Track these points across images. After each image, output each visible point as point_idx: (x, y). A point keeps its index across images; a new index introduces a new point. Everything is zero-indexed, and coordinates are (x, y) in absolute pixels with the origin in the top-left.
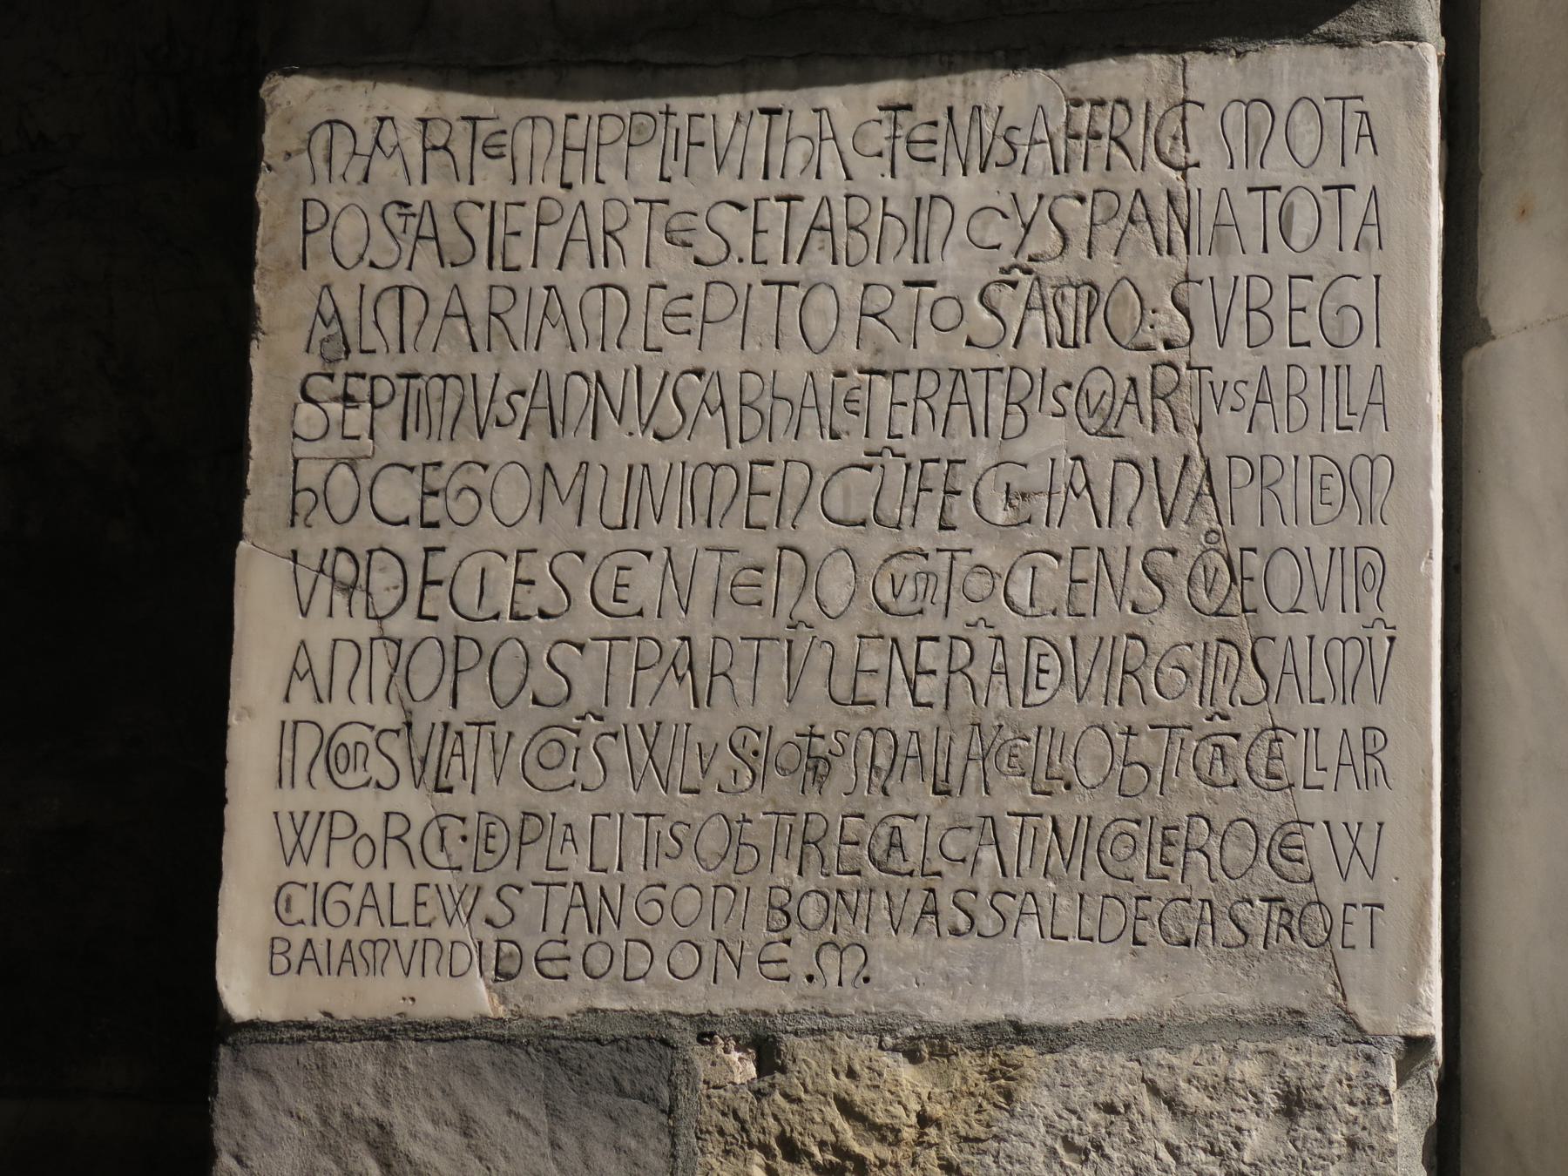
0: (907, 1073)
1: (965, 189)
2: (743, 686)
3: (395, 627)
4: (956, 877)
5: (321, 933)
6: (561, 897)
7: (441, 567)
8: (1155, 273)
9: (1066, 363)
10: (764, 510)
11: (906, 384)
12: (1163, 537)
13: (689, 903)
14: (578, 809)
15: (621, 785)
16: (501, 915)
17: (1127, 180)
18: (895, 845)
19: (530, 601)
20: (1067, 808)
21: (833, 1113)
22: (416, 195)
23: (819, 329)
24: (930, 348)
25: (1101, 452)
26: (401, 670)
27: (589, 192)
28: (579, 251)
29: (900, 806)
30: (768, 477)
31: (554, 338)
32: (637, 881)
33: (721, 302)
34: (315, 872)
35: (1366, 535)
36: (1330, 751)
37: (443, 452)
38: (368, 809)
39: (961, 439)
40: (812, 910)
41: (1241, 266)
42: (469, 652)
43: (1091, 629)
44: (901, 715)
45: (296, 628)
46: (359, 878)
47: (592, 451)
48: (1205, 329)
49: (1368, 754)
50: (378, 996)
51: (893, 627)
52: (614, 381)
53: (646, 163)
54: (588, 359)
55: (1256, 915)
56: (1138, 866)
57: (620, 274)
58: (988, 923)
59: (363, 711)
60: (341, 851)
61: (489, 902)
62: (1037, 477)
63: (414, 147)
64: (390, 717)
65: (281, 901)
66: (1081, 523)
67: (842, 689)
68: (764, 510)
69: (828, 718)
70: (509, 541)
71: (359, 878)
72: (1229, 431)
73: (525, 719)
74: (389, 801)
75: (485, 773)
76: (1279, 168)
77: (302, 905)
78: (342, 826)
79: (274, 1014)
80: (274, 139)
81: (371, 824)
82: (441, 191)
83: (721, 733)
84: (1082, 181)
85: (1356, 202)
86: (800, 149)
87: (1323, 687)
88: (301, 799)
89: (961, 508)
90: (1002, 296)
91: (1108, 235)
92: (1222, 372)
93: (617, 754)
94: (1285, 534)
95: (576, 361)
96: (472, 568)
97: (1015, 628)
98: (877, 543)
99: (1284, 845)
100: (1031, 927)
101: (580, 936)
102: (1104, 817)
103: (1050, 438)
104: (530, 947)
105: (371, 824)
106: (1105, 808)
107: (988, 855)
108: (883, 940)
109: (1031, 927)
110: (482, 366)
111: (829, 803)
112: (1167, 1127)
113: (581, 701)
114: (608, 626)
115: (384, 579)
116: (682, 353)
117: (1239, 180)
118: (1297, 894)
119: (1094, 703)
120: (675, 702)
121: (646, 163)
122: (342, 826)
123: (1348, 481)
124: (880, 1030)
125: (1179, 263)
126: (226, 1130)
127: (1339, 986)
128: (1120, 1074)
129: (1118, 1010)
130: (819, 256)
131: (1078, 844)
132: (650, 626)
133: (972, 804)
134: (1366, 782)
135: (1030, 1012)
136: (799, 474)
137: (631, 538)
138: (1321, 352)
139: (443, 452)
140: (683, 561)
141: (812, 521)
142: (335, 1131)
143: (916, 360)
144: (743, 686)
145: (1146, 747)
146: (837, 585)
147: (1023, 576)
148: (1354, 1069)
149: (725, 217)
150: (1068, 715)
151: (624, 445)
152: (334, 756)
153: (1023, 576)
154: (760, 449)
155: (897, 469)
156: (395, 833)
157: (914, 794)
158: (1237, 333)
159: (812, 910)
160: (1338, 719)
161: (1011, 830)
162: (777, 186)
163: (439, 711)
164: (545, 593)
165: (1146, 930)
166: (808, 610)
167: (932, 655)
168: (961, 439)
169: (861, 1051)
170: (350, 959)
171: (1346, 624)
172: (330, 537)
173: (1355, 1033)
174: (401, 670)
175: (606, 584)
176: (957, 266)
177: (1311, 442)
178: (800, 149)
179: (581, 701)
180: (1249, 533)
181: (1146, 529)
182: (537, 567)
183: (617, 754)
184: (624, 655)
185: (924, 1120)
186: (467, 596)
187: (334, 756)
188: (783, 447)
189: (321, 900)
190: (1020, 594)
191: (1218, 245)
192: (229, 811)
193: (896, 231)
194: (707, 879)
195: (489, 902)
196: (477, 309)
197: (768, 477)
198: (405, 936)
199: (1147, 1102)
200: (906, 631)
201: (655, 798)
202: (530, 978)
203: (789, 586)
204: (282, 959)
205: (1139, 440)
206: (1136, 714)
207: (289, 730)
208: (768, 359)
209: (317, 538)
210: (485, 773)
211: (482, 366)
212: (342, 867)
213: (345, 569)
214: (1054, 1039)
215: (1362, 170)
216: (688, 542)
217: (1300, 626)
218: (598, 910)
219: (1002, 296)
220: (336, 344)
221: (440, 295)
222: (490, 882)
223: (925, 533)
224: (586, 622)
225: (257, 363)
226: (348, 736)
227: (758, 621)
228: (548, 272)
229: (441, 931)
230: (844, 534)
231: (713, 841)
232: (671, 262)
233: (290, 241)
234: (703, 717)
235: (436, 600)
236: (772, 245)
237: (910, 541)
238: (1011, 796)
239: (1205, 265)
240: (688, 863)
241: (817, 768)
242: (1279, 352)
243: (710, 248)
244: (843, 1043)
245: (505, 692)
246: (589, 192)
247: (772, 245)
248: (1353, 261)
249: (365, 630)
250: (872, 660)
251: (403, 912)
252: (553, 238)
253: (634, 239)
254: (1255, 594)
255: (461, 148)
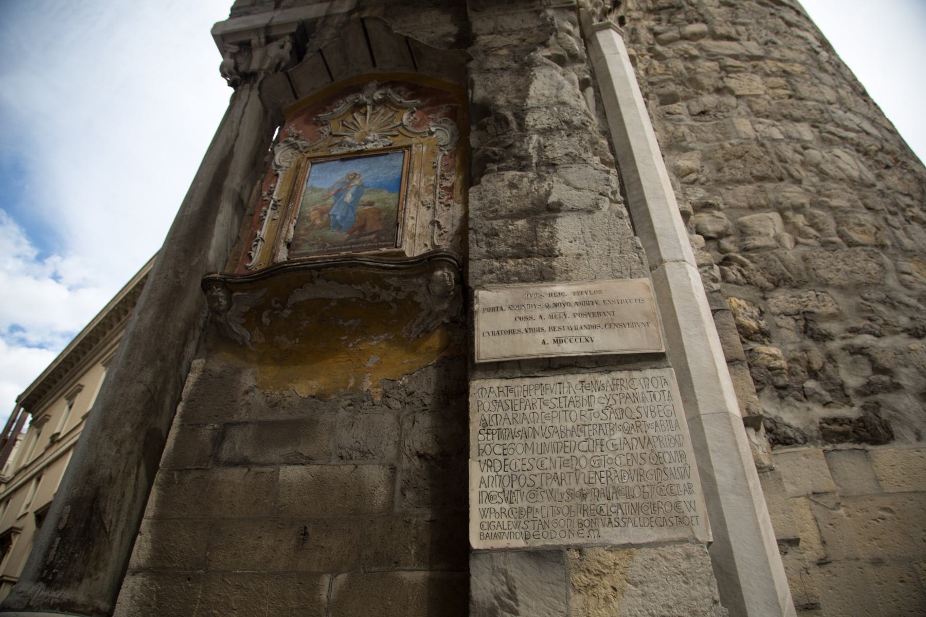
0: (610, 554)
1: (597, 394)
2: (568, 481)
3: (500, 473)
4: (614, 516)
5: (490, 531)
6: (537, 523)
7: (507, 462)
8: (633, 406)
9: (619, 422)
10: (567, 450)
11: (591, 427)
12: (643, 451)
13: (562, 523)
14: (538, 506)
15: (546, 501)
16: (525, 526)
17: (625, 391)
18: (601, 510)
19: (525, 468)
20: (634, 501)
21: (597, 563)
22: (498, 399)
23: (573, 418)
24: (594, 421)
25: (629, 437)
26: (502, 481)
27: (528, 397)
28: (528, 407)
29: (601, 502)
30: (568, 444)
31: (525, 422)
32: (551, 519)
33: (555, 415)
34: (488, 519)
35: (680, 449)
36: (682, 488)
37: (506, 442)
38: (497, 507)
39: (602, 436)
40: (587, 523)
41: (648, 404)
42: (514, 477)
43: (633, 468)
44: (598, 486)
45: (481, 474)
46: (497, 521)
47: (534, 441)
48: (644, 415)
49: (689, 488)
50: (502, 543)
51: (595, 469)
52: (537, 428)
53: (539, 392)
54: (531, 425)
55: (674, 520)
56: (649, 512)
57: (536, 411)
58: (622, 524)
59: (495, 489)
60: (493, 515)
61: (522, 525)
62: (617, 442)
63: (497, 392)
64: (500, 490)
65: (481, 526)
66: (627, 449)
67: (587, 481)
68: (567, 450)
69: (585, 487)
70: (520, 457)
71: (497, 521)
72: (651, 432)
73: (526, 490)
74: (501, 506)
75: (519, 500)
76: (651, 388)
77: (486, 526)
78: (492, 511)
79: (481, 547)
80: (472, 391)
81: (498, 510)
82: (502, 398)
83: (564, 490)
84: (616, 392)
85: (666, 393)
86: (566, 390)
87: (678, 476)
88: (484, 506)
89: (604, 448)
90: (606, 411)
91: (623, 400)
92: (648, 422)
93: (545, 495)
94: (666, 449)
95: (530, 425)
96: (513, 462)
97: (618, 469)
98: (589, 455)
99: (677, 505)
100: (630, 524)
101: (541, 531)
102: (641, 502)
103: (618, 435)
104: (531, 532)
105: (498, 510)
106: (641, 501)
107: (620, 511)
108: (601, 529)
109: (630, 524)
110: (512, 427)
111: (587, 502)
112: (665, 563)
113: (537, 485)
114: (540, 472)
115: (497, 465)
116: (549, 423)
117: (645, 390)
118: (681, 515)
119: (635, 482)
120: (555, 485)
121: (539, 392)
122: (492, 511)
123: (675, 439)
124: (603, 546)
125: (637, 404)
126: (473, 571)
127: (693, 532)
128: (653, 552)
129: (651, 540)
130: (571, 406)
131: (637, 508)
132: (548, 471)
133: (615, 501)
134: (690, 493)
135: (633, 541)
136: (573, 443)
137: (543, 456)
138: (665, 418)
139: (506, 442)
140: (553, 459)
141: (577, 451)
142: (494, 571)
143: (592, 423)
144: (568, 481)
145: (647, 489)
146: (583, 462)
147: (618, 459)
148: (699, 549)
149: (554, 400)
150: (631, 484)
151: (539, 440)
152: (490, 497)
153: (618, 459)
154: (565, 439)
155: (591, 442)
156: (503, 511)
157: (603, 500)
158: (650, 415)
159: (587, 523)
160: (682, 482)
161: (623, 506)
162: (562, 395)
163: (509, 488)
164: (528, 466)
165: (653, 524)
166: (578, 467)
167: (603, 474)
168: (602, 436)
169: (601, 551)
170: (496, 536)
171: (681, 465)
172: (486, 458)
173: (697, 541)
174: (502, 481)
175: (539, 464)
176: (597, 407)
177: (667, 433)
178: (566, 390)
179: (537, 485)
180: (659, 450)
181: (639, 450)
182: (525, 461)
183: (545, 495)
184: (544, 478)
185: (616, 564)
186: (513, 467)
187: (490, 497)
188: (570, 438)
189: (489, 525)
190: (618, 462)
191: (644, 401)
192: (470, 509)
193: (585, 402)
194: (565, 518)
195: (522, 525)
196: (510, 417)
197: (568, 444)
198: (507, 532)
199: (660, 558)
200: (598, 470)
201: (554, 503)
202: (532, 539)
203: (574, 463)
204: (482, 537)
205: (635, 434)
206: (644, 483)
207: (481, 493)
208: (564, 424)
209: (484, 458)
210: (519, 500)
211: (512, 427)
212: (493, 518)
213: (489, 463)
214: (639, 546)
215: (666, 388)
216: (554, 456)
217: (672, 466)
218: (545, 525)
219: (606, 411)
220: (485, 424)
221: (504, 416)
222: (522, 521)
223: (598, 452)
224: (536, 471)
225: (471, 428)
226: (492, 494)
227: (569, 470)
228: (522, 411)
229: (513, 530)
230: (584, 454)
231: (565, 511)
232: (545, 409)
233: (475, 407)
234: (561, 488)
235: (507, 468)
236: (563, 405)
237: (596, 454)
238: (622, 500)
239: (642, 404)
240: (561, 515)
241: (584, 496)
242: (658, 418)
243: (552, 406)
244: (597, 549)
245: (522, 484)
246: (528, 397)
247: (563, 405)
248: (668, 403)
249: (494, 474)
250: (592, 476)
251: (506, 527)
252: (523, 405)
253: (538, 405)
254: (662, 460)
255: (505, 391)
